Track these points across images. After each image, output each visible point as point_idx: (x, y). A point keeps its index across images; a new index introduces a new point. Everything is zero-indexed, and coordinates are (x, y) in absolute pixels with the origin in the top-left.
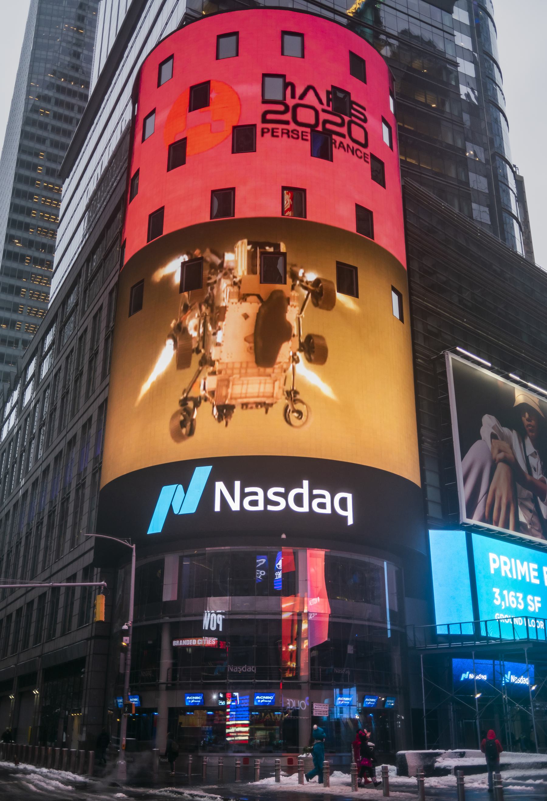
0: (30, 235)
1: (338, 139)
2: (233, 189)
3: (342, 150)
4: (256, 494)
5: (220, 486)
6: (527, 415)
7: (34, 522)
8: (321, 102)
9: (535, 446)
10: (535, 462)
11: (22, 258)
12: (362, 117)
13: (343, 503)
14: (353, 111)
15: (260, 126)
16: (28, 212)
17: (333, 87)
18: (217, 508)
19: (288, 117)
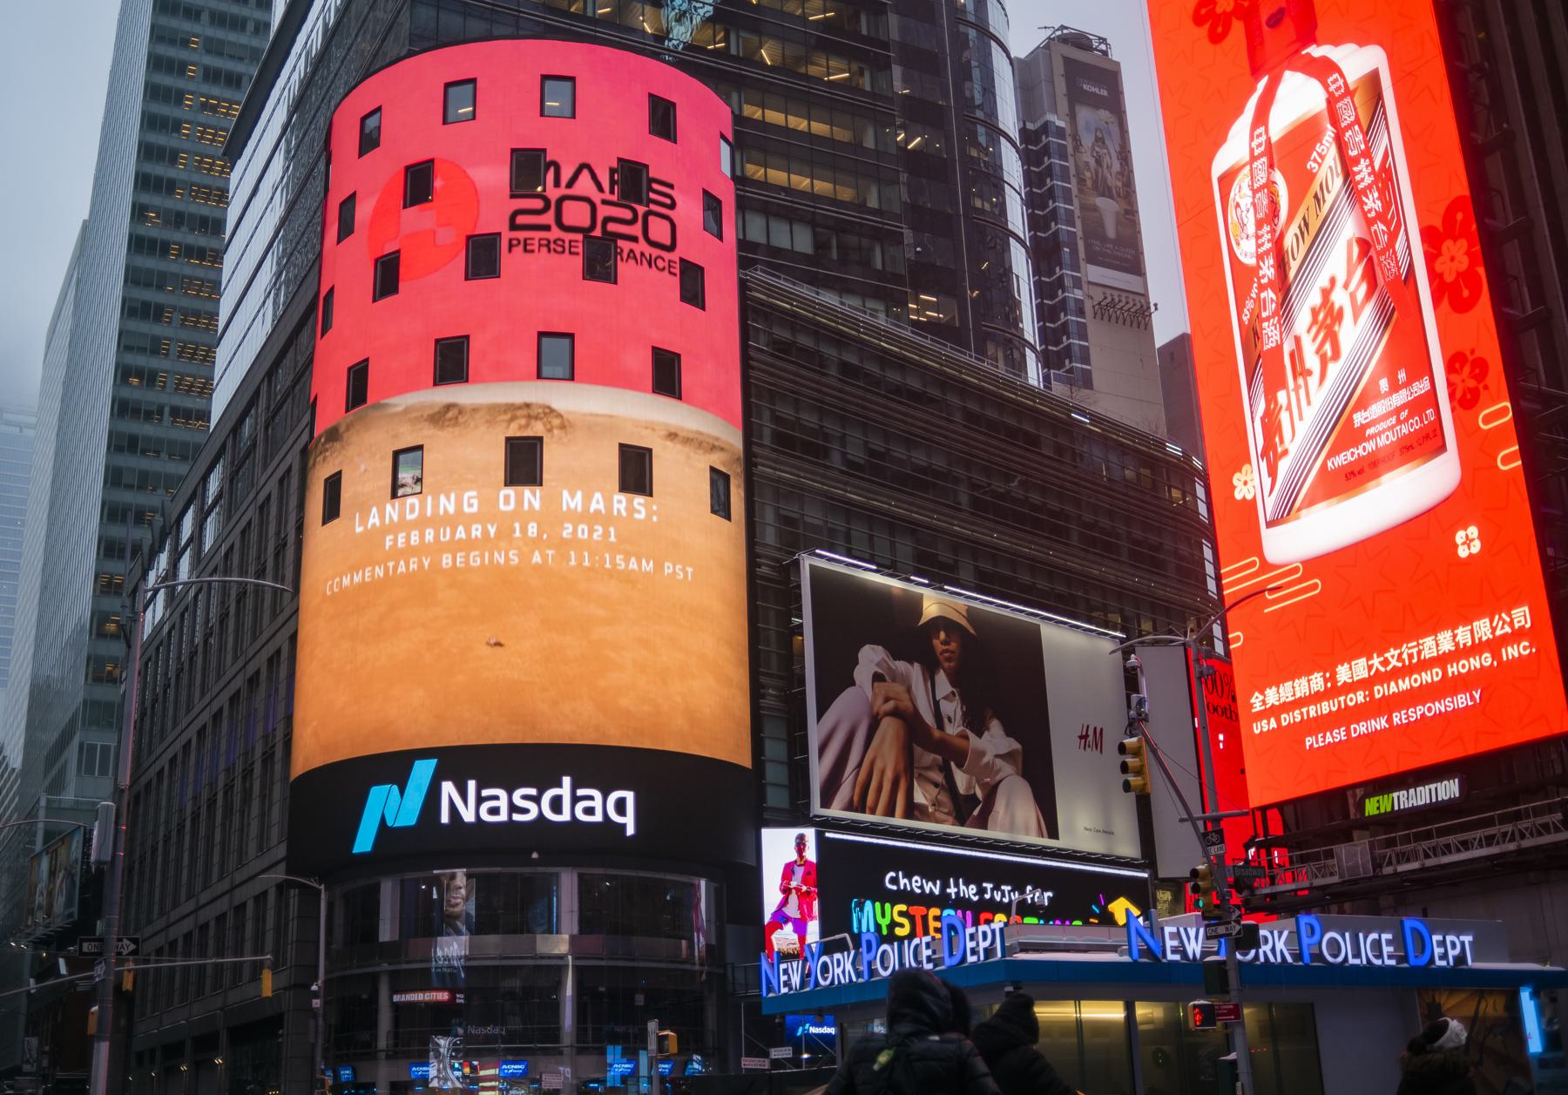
0: (177, 202)
1: (625, 245)
2: (467, 337)
3: (632, 262)
4: (496, 798)
5: (448, 788)
6: (942, 635)
7: (205, 796)
8: (601, 189)
9: (953, 684)
10: (952, 708)
11: (164, 248)
12: (668, 201)
13: (621, 807)
14: (652, 196)
15: (507, 235)
16: (173, 157)
17: (620, 160)
18: (445, 819)
19: (549, 218)
